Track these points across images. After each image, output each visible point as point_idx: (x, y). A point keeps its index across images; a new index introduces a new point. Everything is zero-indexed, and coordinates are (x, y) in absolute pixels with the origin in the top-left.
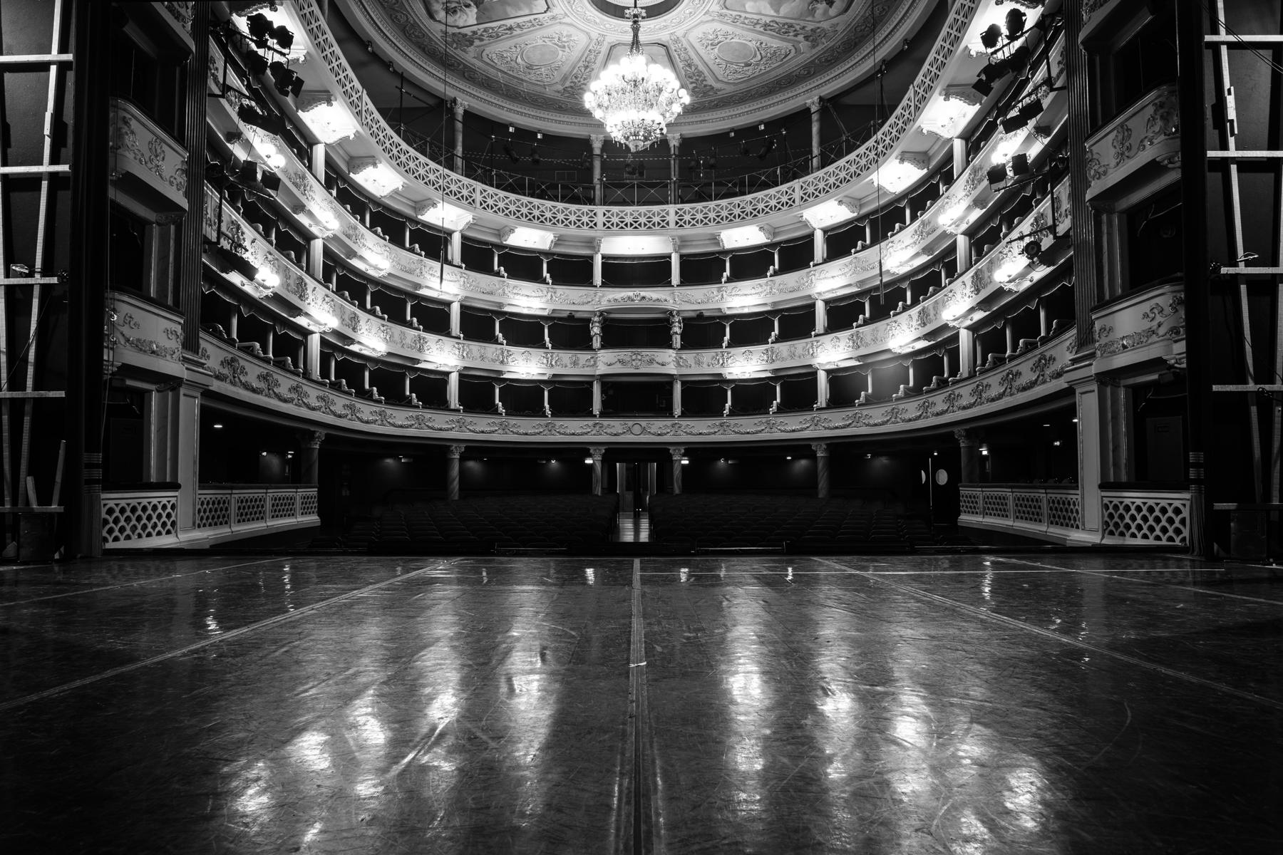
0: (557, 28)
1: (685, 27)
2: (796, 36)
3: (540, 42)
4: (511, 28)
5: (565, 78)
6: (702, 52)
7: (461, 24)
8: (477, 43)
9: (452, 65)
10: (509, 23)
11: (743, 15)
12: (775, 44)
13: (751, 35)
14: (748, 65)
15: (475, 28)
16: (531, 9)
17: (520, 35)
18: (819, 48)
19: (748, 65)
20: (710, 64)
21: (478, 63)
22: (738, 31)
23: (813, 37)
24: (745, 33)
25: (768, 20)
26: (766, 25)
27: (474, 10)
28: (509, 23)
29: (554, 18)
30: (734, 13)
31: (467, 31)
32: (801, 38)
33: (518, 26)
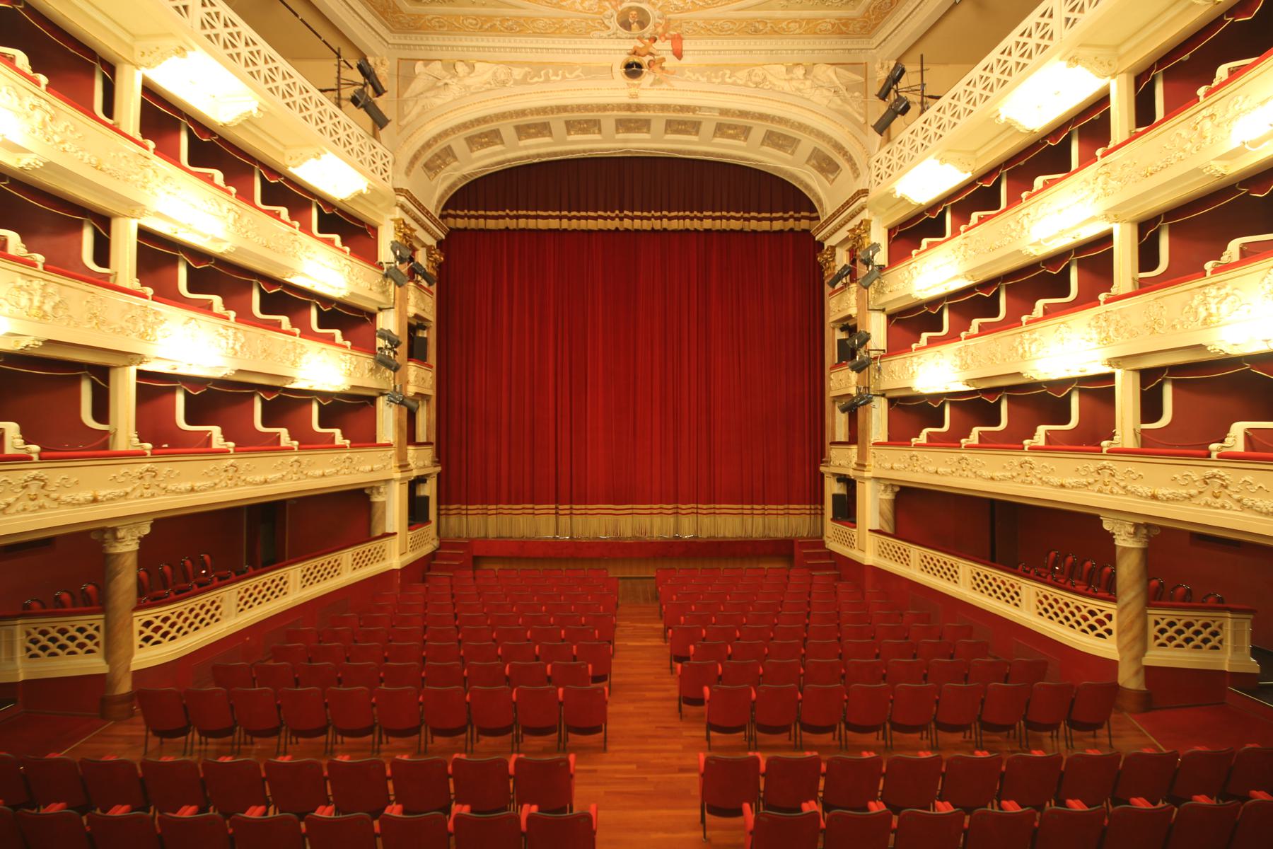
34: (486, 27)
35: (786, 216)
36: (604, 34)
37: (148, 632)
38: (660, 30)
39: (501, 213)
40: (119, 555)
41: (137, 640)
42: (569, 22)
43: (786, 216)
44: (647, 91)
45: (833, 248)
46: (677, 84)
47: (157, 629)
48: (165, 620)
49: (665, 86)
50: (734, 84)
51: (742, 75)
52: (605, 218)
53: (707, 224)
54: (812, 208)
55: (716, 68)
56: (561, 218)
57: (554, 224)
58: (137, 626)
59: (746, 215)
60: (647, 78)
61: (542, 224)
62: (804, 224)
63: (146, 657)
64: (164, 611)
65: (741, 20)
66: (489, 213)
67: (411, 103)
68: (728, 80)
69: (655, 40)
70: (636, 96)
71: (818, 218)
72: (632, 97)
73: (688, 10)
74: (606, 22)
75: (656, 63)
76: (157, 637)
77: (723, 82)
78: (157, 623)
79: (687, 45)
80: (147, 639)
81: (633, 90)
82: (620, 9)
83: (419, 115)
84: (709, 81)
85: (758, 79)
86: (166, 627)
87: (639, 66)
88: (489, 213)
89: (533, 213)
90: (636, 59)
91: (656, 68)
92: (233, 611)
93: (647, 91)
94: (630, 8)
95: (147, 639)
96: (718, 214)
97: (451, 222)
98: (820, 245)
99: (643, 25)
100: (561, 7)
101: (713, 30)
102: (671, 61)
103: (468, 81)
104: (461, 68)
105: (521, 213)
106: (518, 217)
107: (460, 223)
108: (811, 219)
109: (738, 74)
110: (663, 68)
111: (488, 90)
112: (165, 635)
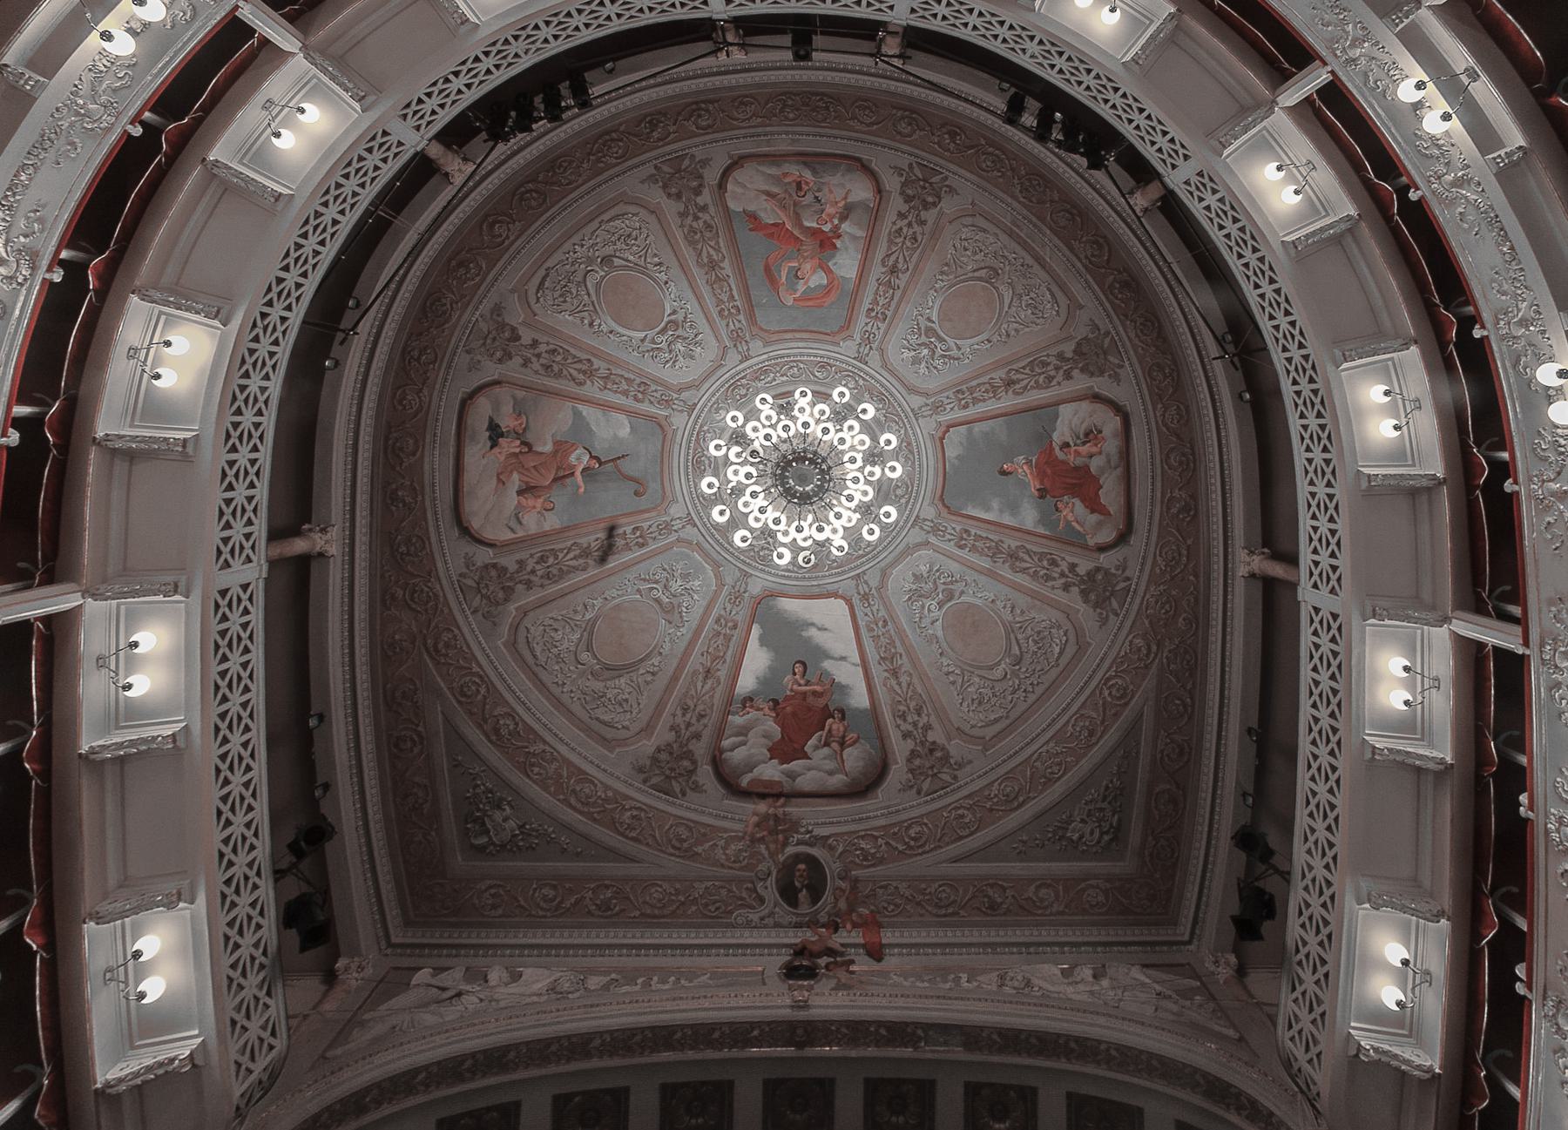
0: (931, 385)
1: (725, 375)
2: (535, 343)
3: (965, 344)
4: (1009, 383)
5: (935, 235)
6: (692, 305)
7: (1085, 406)
8: (1068, 349)
9: (1125, 285)
10: (1008, 401)
11: (628, 402)
12: (565, 322)
13: (610, 347)
14: (606, 260)
15: (1068, 388)
16: (970, 431)
17: (997, 366)
18: (486, 306)
19: (606, 260)
20: (675, 271)
21: (1082, 296)
22: (633, 358)
23: (503, 340)
24: (623, 356)
25: (591, 389)
26: (590, 373)
27: (1055, 436)
28: (1008, 401)
29: (937, 408)
30: (645, 407)
31: (1081, 382)
32: (526, 336)
33: (994, 389)
34: (567, 904)
36: (755, 917)
38: (842, 905)
42: (700, 887)
74: (759, 885)
79: (888, 937)
82: (781, 858)
94: (797, 858)
99: (816, 893)
100: (695, 856)
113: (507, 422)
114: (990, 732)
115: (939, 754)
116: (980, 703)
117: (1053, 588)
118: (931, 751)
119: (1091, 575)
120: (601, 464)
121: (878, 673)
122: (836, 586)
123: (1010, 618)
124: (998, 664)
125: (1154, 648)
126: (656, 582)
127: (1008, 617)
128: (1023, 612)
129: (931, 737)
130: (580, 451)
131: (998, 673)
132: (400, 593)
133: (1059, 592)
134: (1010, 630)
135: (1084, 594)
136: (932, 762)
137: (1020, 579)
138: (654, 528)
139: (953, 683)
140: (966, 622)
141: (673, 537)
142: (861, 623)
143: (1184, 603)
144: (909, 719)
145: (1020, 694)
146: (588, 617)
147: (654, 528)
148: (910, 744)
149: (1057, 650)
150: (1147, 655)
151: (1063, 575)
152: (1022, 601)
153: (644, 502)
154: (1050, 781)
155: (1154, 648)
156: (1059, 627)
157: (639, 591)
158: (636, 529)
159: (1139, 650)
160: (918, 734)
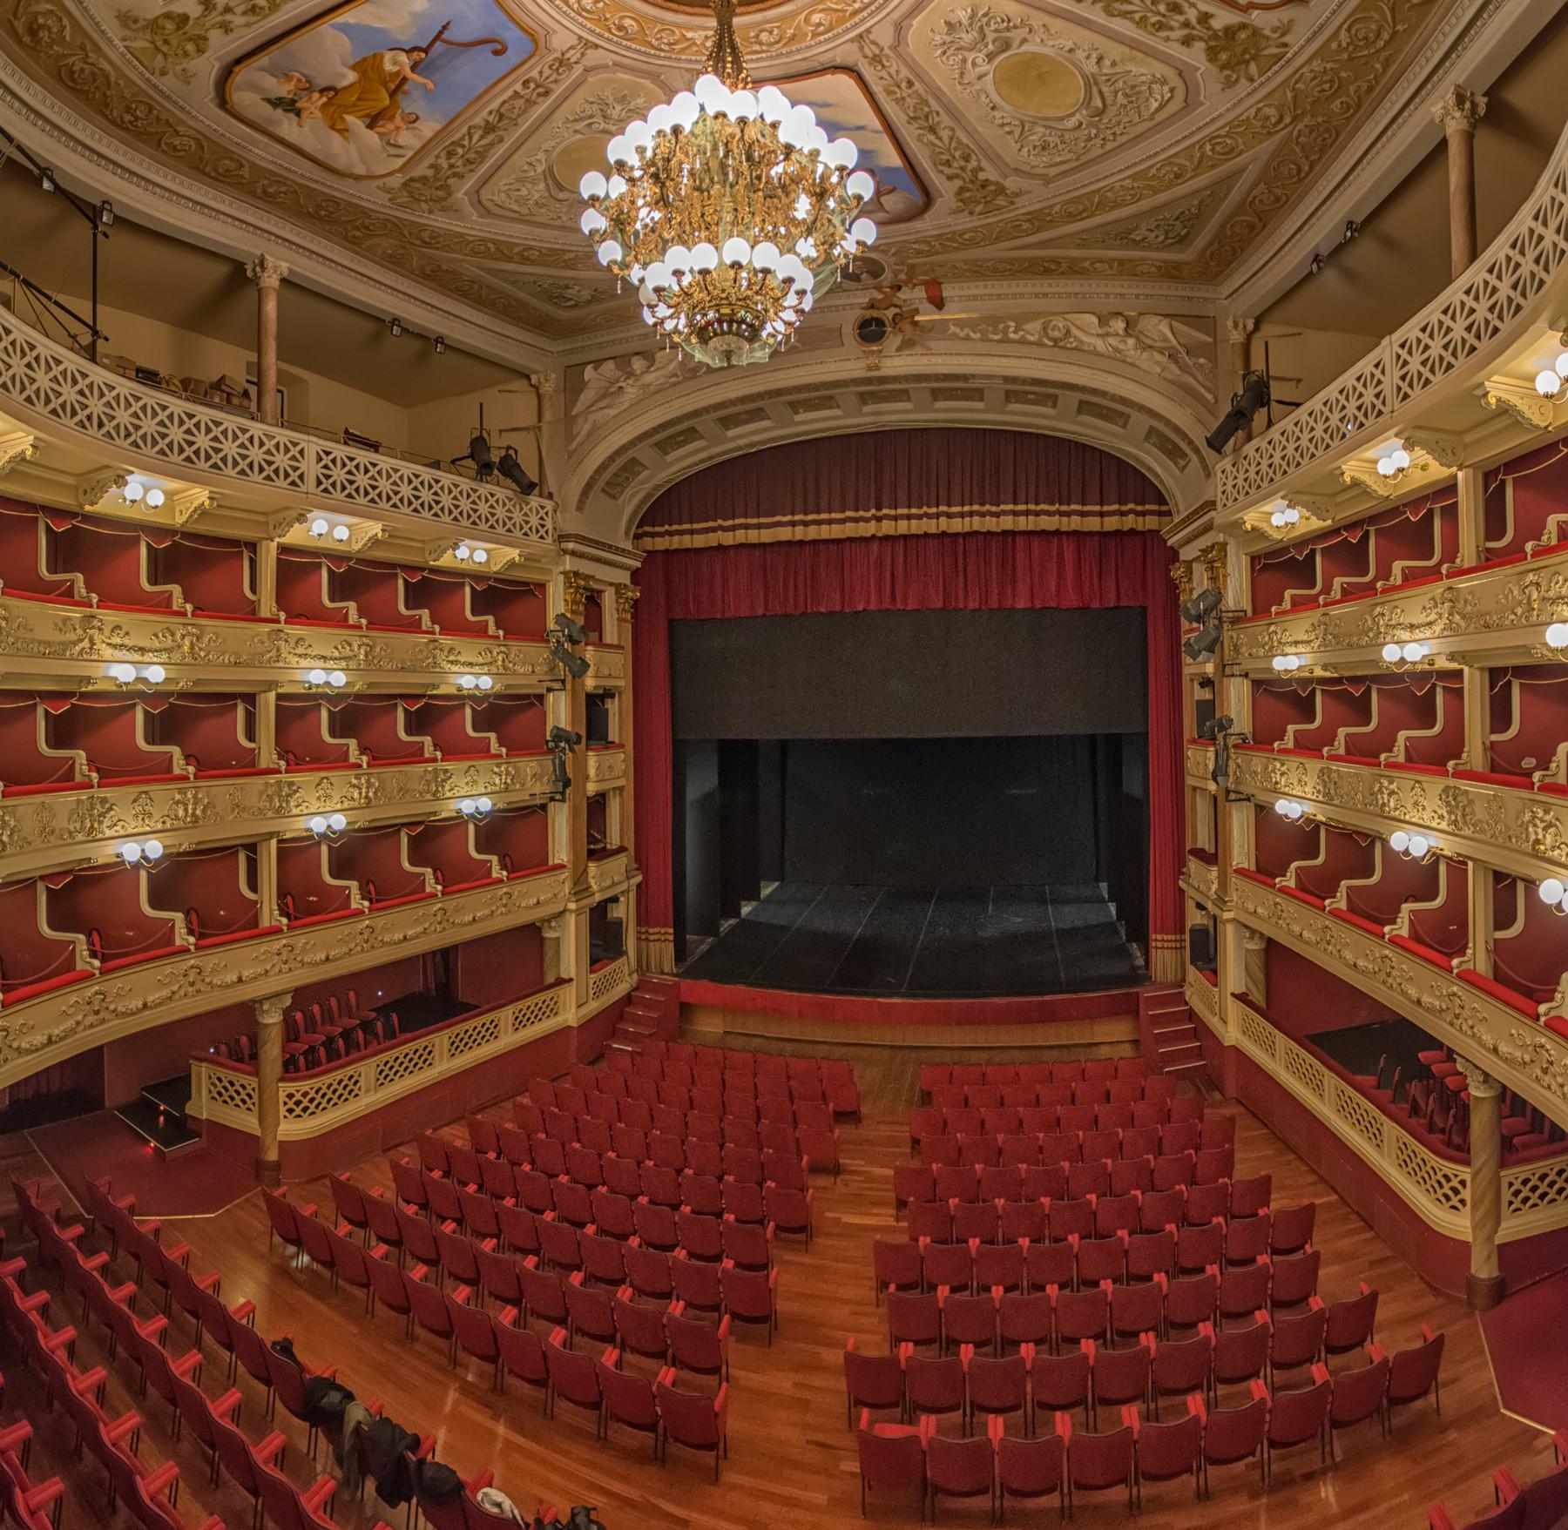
35: (1124, 508)
37: (291, 1104)
38: (903, 276)
39: (711, 524)
40: (266, 1025)
41: (283, 1110)
43: (1124, 508)
44: (897, 362)
45: (1189, 564)
46: (936, 345)
47: (298, 1103)
48: (305, 1094)
49: (918, 349)
50: (1023, 342)
51: (1033, 329)
52: (856, 520)
53: (1007, 523)
54: (1161, 500)
55: (994, 321)
56: (793, 524)
57: (784, 534)
58: (282, 1096)
59: (1064, 508)
60: (893, 341)
61: (766, 536)
62: (1151, 523)
63: (291, 1129)
64: (305, 1086)
65: (1016, 260)
66: (695, 526)
67: (580, 421)
68: (1012, 336)
69: (899, 288)
70: (878, 368)
71: (1169, 513)
72: (870, 368)
73: (937, 253)
75: (905, 317)
76: (298, 1111)
77: (1006, 340)
78: (298, 1096)
79: (948, 291)
80: (290, 1111)
81: (872, 360)
83: (589, 435)
84: (985, 339)
85: (1056, 334)
86: (305, 1103)
87: (880, 323)
88: (695, 526)
89: (754, 521)
90: (875, 313)
91: (906, 326)
92: (373, 1086)
93: (897, 362)
95: (290, 1111)
96: (1022, 507)
97: (648, 543)
98: (1173, 555)
101: (978, 271)
102: (927, 316)
103: (648, 378)
104: (638, 364)
105: (738, 521)
106: (733, 528)
107: (661, 544)
108: (1160, 514)
109: (1028, 327)
110: (916, 324)
111: (675, 384)
112: (305, 1109)
113: (284, 90)
114: (1053, 172)
115: (992, 188)
116: (1044, 148)
117: (1167, 39)
118: (983, 187)
119: (1230, 33)
120: (426, 51)
121: (909, 134)
122: (829, 55)
123: (1094, 69)
124: (1072, 115)
125: (1287, 120)
126: (591, 117)
127: (1091, 67)
128: (1114, 64)
129: (982, 176)
130: (388, 56)
131: (1072, 123)
132: (357, 233)
133: (1177, 45)
134: (1090, 82)
135: (1212, 54)
136: (980, 192)
137: (1118, 24)
138: (547, 72)
139: (1009, 133)
140: (1028, 75)
141: (578, 71)
142: (877, 89)
143: (1352, 89)
144: (955, 164)
145: (1098, 142)
146: (540, 169)
147: (547, 72)
148: (958, 183)
149: (1155, 105)
150: (1275, 125)
151: (1186, 24)
152: (1115, 51)
153: (511, 57)
154: (1117, 206)
155: (1287, 120)
156: (1164, 82)
157: (576, 132)
158: (526, 84)
159: (1268, 118)
160: (968, 176)
